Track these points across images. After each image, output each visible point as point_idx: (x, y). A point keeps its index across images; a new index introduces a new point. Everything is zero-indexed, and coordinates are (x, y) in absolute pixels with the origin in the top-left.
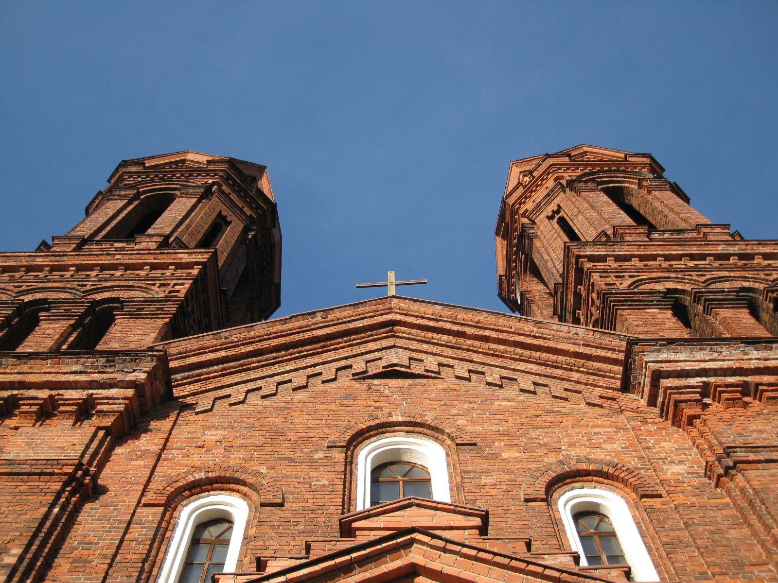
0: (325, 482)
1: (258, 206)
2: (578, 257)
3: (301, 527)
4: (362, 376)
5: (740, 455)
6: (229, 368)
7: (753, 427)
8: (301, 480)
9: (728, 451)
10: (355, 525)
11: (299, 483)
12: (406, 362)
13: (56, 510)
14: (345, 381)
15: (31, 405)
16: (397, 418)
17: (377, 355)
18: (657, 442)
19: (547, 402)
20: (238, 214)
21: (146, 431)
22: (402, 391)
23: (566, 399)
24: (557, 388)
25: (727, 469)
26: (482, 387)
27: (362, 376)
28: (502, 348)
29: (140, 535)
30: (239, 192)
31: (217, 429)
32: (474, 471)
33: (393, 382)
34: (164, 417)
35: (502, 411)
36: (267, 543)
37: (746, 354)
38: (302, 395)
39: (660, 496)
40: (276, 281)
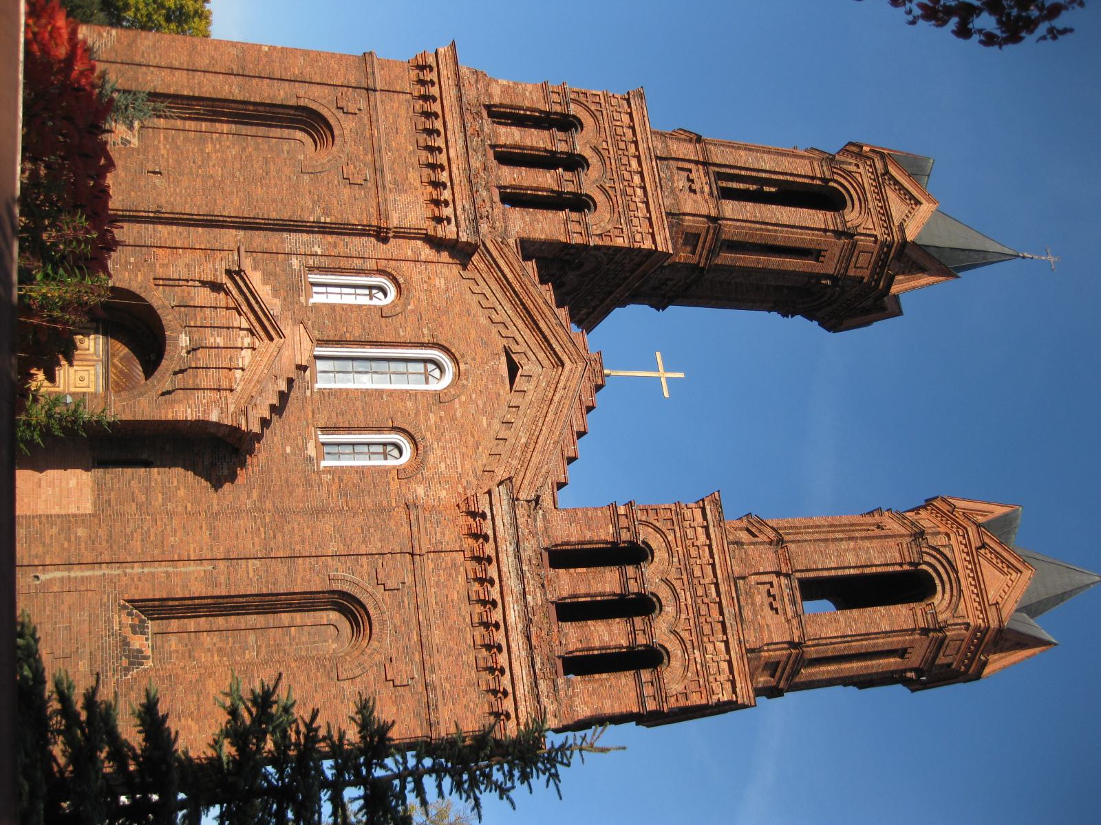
1: (878, 281)
3: (367, 325)
6: (502, 281)
7: (446, 532)
13: (360, 227)
16: (462, 367)
20: (841, 265)
21: (438, 252)
22: (495, 371)
29: (358, 263)
34: (451, 256)
37: (510, 544)
38: (484, 321)
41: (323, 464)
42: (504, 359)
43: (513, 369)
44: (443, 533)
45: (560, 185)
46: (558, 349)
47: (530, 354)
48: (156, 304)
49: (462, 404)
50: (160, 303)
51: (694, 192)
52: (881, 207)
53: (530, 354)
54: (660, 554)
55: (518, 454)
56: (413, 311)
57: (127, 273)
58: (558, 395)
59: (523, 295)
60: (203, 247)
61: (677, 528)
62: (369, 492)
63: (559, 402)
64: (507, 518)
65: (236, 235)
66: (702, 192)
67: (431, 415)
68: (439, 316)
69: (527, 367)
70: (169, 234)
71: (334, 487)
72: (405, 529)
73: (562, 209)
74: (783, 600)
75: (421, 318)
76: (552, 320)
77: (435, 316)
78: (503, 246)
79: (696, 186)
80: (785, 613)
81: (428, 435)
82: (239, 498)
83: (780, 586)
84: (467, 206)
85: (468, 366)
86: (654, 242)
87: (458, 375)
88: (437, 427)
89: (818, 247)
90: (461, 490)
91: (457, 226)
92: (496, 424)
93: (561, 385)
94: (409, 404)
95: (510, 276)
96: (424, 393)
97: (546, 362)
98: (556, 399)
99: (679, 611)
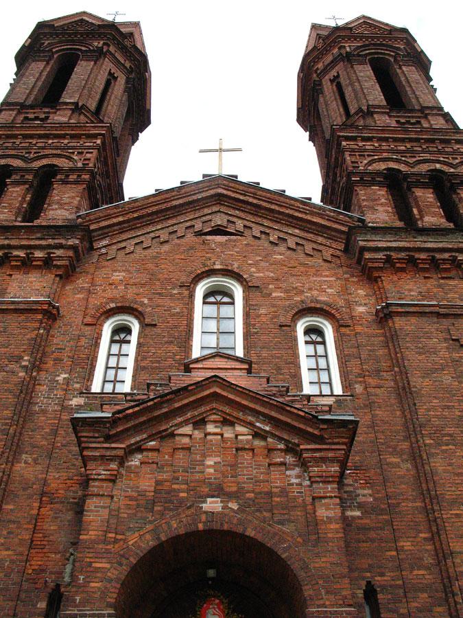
0: (178, 310)
1: (136, 59)
2: (339, 136)
3: (166, 339)
4: (200, 234)
5: (394, 309)
8: (166, 308)
9: (388, 305)
10: (191, 366)
11: (165, 310)
12: (225, 224)
14: (190, 237)
15: (16, 261)
16: (218, 267)
17: (209, 217)
18: (356, 289)
19: (301, 257)
22: (221, 244)
23: (312, 256)
24: (309, 247)
25: (386, 315)
26: (267, 244)
27: (200, 234)
28: (281, 217)
30: (122, 48)
31: (120, 272)
32: (256, 305)
33: (219, 238)
35: (275, 263)
36: (150, 349)
37: (415, 238)
38: (166, 247)
39: (350, 326)
40: (148, 107)
41: (338, 390)
42: (209, 237)
43: (218, 231)
44: (410, 290)
45: (25, 183)
46: (204, 195)
47: (204, 219)
48: (149, 542)
49: (259, 271)
50: (148, 536)
51: (47, 118)
52: (81, 36)
53: (204, 219)
54: (392, 165)
55: (312, 235)
56: (150, 299)
57: (92, 585)
58: (251, 200)
59: (144, 212)
60: (36, 505)
61: (366, 153)
62: (370, 351)
63: (259, 199)
64: (388, 238)
65: (26, 462)
66: (49, 113)
67: (274, 295)
68: (159, 280)
69: (219, 220)
70: (7, 549)
71: (371, 381)
72: (413, 320)
73: (51, 183)
74: (409, 117)
75: (159, 294)
76: (173, 194)
77: (158, 283)
78: (87, 219)
79: (43, 116)
80: (419, 117)
81: (298, 299)
82: (400, 477)
83: (398, 117)
84: (39, 235)
85: (217, 263)
86: (95, 136)
87: (227, 273)
88: (286, 291)
89: (107, 74)
90: (355, 279)
91: (60, 246)
92: (282, 248)
93: (241, 197)
94: (262, 311)
95: (121, 219)
96: (246, 299)
97: (215, 209)
98: (255, 201)
99: (439, 162)
